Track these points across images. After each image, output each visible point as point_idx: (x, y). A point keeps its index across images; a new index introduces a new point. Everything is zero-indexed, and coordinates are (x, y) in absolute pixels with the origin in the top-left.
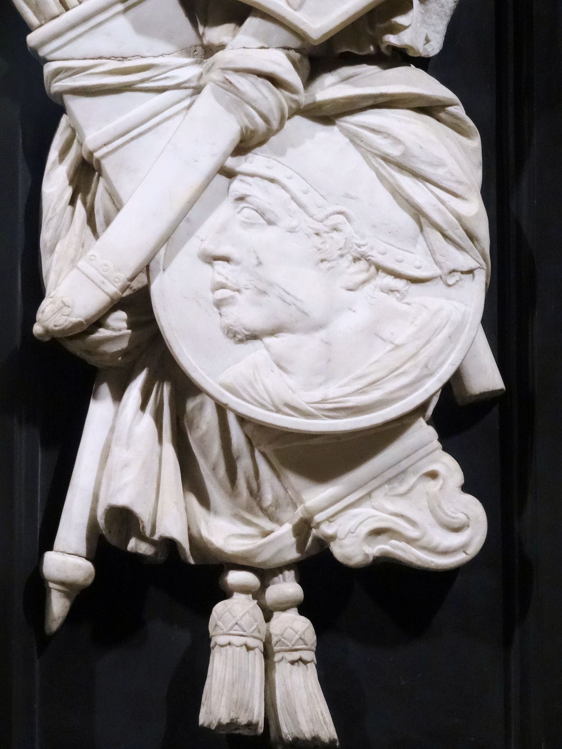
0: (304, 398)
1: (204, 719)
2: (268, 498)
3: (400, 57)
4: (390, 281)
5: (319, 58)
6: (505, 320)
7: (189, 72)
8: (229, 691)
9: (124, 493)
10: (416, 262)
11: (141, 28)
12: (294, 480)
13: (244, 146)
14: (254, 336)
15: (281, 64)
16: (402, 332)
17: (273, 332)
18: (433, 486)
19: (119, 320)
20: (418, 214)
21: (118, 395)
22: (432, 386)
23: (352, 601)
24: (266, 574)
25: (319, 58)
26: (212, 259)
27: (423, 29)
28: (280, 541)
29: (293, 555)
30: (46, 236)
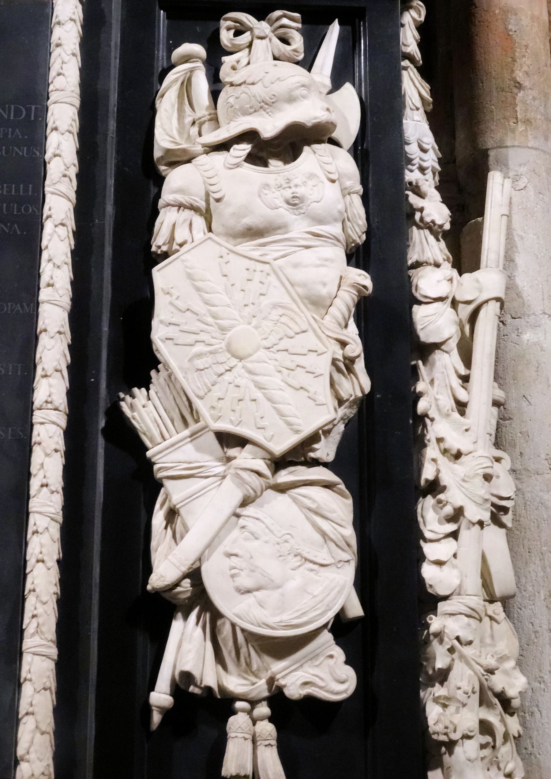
0: (272, 620)
1: (224, 773)
2: (255, 667)
3: (315, 463)
4: (311, 566)
5: (279, 463)
6: (364, 583)
7: (220, 469)
10: (323, 556)
11: (199, 449)
12: (267, 659)
13: (244, 503)
14: (249, 591)
15: (262, 466)
16: (317, 590)
17: (258, 589)
18: (331, 662)
19: (187, 583)
20: (324, 534)
21: (186, 617)
22: (330, 615)
23: (293, 716)
24: (253, 703)
25: (279, 463)
26: (230, 555)
27: (326, 450)
28: (261, 688)
29: (266, 694)
30: (153, 544)
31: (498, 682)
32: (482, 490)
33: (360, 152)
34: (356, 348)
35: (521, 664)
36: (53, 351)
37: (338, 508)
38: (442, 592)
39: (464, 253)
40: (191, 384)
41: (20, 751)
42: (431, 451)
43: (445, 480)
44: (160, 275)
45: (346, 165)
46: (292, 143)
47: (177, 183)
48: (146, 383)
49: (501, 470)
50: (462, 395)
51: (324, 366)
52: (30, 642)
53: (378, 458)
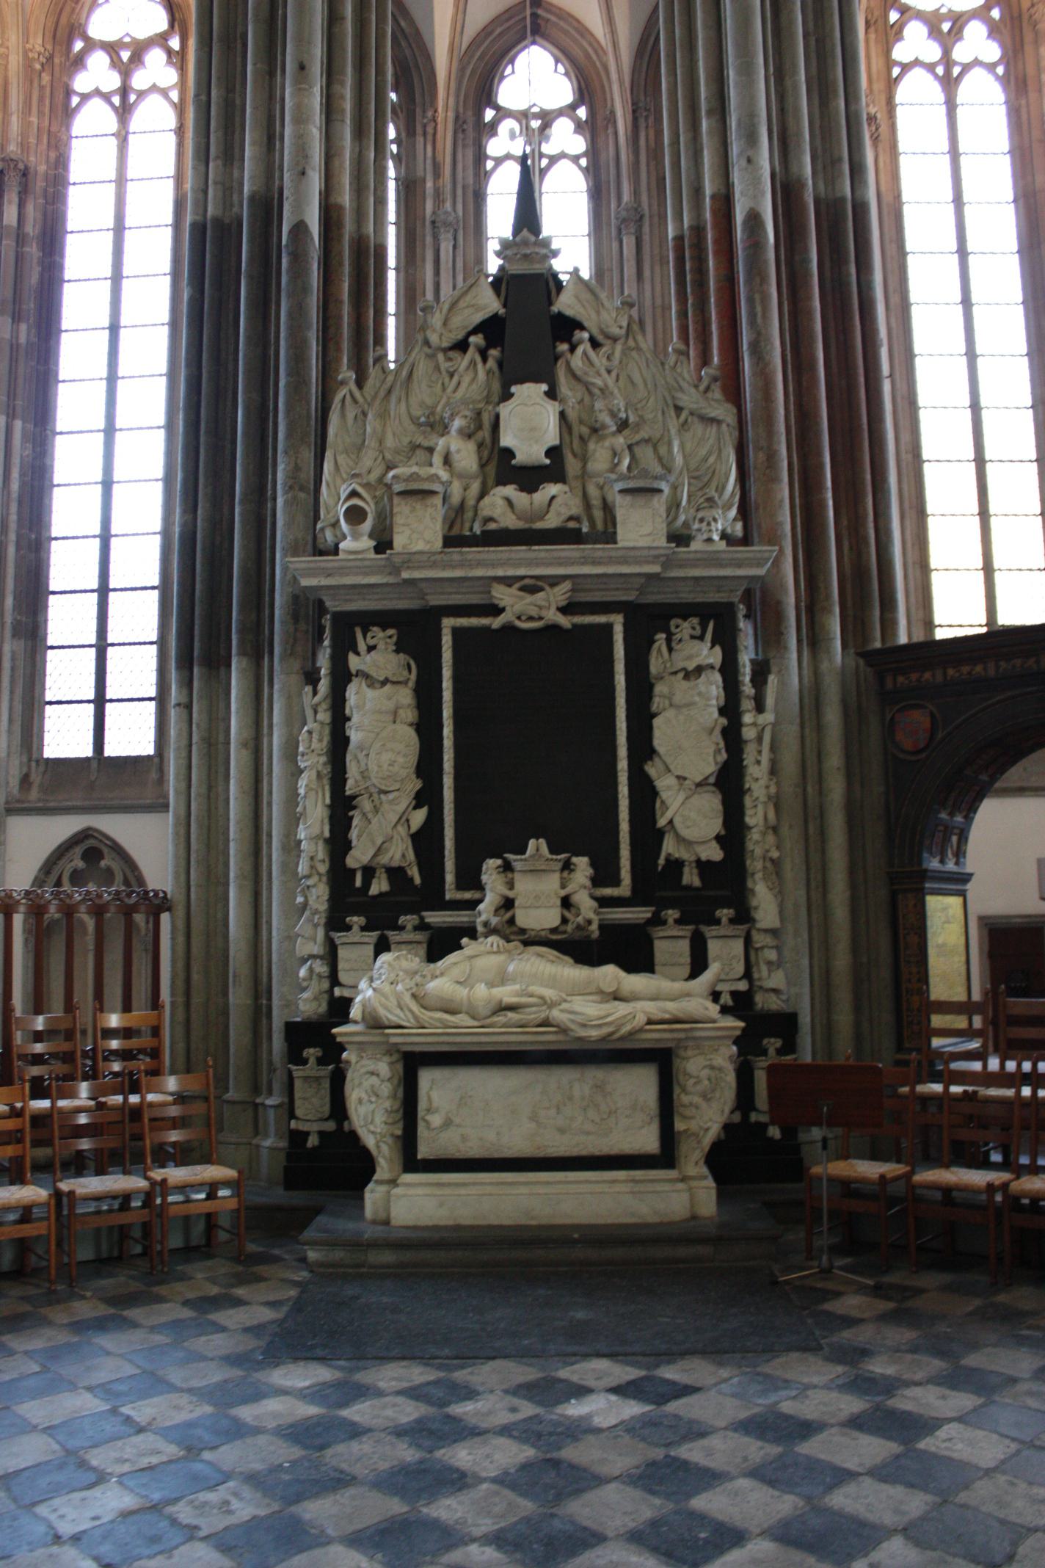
6: (726, 824)
8: (686, 879)
9: (670, 851)
23: (704, 867)
27: (712, 780)
28: (693, 858)
31: (770, 854)
33: (723, 670)
34: (722, 745)
35: (778, 848)
36: (622, 752)
39: (760, 708)
40: (668, 760)
42: (748, 778)
44: (657, 722)
45: (718, 677)
46: (699, 670)
47: (659, 689)
48: (651, 759)
51: (711, 750)
53: (729, 782)
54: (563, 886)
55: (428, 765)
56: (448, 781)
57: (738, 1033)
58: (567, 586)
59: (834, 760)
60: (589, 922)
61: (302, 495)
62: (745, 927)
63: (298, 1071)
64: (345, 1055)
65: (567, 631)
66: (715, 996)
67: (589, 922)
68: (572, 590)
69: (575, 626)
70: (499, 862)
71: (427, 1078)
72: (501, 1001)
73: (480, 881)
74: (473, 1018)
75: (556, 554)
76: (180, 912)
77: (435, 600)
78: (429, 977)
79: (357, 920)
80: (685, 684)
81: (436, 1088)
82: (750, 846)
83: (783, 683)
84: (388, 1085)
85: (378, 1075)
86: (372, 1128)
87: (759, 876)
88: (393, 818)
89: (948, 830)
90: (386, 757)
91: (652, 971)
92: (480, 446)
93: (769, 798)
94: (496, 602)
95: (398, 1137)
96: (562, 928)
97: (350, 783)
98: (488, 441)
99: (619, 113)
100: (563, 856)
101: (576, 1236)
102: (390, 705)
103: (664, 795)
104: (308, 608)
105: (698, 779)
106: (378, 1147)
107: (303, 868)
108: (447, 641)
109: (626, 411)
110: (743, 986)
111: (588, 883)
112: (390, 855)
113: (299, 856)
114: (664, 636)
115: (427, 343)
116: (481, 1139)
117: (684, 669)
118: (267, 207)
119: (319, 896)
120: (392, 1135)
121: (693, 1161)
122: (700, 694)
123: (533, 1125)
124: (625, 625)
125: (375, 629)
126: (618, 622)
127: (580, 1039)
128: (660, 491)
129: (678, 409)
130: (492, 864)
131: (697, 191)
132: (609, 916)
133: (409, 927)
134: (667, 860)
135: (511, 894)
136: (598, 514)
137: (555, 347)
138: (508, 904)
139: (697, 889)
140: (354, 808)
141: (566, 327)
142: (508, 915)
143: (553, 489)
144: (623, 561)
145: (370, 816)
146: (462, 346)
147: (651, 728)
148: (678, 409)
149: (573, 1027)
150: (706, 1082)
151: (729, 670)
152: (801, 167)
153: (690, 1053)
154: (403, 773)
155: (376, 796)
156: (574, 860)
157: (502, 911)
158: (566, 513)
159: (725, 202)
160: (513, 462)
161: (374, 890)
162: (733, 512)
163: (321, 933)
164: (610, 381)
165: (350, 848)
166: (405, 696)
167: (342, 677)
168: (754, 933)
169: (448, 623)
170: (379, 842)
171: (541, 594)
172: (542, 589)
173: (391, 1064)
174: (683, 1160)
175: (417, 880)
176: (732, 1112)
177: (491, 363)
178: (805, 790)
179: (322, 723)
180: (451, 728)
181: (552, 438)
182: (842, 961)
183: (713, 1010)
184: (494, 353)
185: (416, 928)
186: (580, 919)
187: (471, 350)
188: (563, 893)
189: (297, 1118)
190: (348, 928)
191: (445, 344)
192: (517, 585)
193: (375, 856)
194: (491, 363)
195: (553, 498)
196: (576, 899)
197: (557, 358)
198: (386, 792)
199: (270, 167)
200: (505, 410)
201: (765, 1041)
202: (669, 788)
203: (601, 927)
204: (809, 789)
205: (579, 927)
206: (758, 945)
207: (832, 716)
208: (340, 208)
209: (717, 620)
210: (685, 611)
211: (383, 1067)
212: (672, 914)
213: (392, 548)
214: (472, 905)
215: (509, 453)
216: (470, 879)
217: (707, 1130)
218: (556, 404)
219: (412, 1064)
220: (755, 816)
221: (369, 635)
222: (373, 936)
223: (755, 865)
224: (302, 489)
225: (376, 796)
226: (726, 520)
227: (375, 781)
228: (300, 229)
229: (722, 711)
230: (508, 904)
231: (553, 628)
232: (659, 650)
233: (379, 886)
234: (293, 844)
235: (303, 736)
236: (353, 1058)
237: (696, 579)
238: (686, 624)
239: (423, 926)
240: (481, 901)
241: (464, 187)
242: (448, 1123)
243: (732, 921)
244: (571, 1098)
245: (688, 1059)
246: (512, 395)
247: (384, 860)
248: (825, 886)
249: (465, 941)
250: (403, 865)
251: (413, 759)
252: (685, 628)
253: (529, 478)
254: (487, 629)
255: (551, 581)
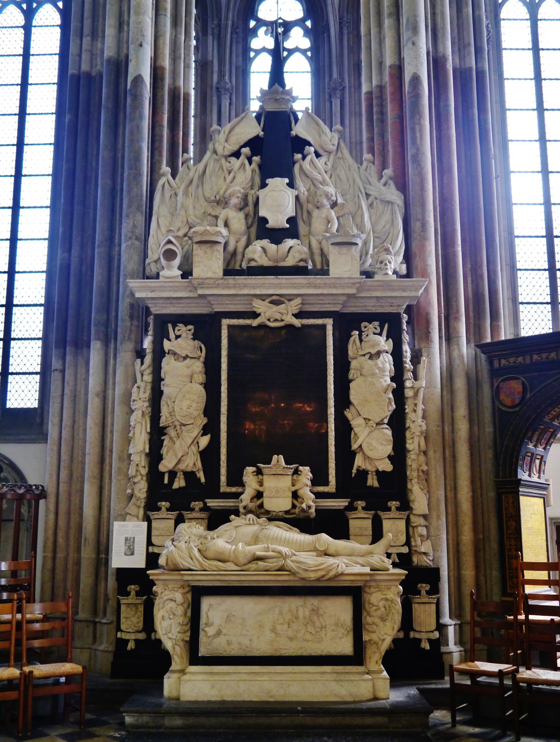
6: (394, 449)
9: (360, 465)
23: (380, 474)
27: (386, 421)
28: (374, 469)
31: (421, 468)
32: (419, 429)
37: (389, 432)
38: (410, 450)
39: (416, 378)
41: (330, 480)
43: (411, 426)
44: (352, 385)
46: (379, 353)
49: (423, 424)
50: (415, 408)
52: (330, 461)
53: (398, 422)
54: (293, 485)
55: (211, 409)
56: (224, 419)
57: (403, 577)
58: (298, 301)
59: (461, 411)
60: (309, 507)
61: (137, 243)
62: (407, 513)
63: (124, 601)
64: (155, 588)
65: (299, 328)
66: (389, 556)
67: (309, 507)
68: (302, 304)
69: (303, 326)
70: (254, 469)
71: (206, 603)
72: (255, 554)
73: (242, 481)
74: (237, 565)
75: (292, 281)
76: (52, 499)
77: (218, 309)
78: (210, 538)
79: (164, 504)
80: (370, 362)
81: (213, 609)
82: (409, 462)
83: (430, 363)
84: (182, 607)
85: (175, 601)
86: (170, 635)
87: (415, 481)
88: (190, 441)
89: (533, 457)
90: (185, 404)
91: (349, 539)
92: (247, 216)
93: (422, 432)
94: (255, 310)
95: (186, 641)
96: (293, 511)
97: (163, 419)
98: (252, 213)
99: (332, 23)
100: (294, 465)
101: (299, 708)
102: (188, 372)
103: (356, 430)
104: (141, 311)
105: (378, 420)
106: (174, 648)
107: (132, 471)
108: (224, 333)
109: (336, 196)
110: (405, 550)
111: (309, 483)
112: (186, 464)
113: (129, 464)
114: (357, 332)
115: (215, 152)
116: (239, 643)
117: (370, 353)
118: (120, 66)
119: (141, 489)
120: (183, 640)
121: (374, 659)
122: (379, 368)
123: (273, 635)
124: (333, 326)
125: (180, 325)
126: (329, 323)
127: (303, 579)
128: (357, 244)
129: (368, 195)
130: (250, 470)
131: (381, 64)
132: (321, 504)
133: (197, 509)
134: (357, 470)
135: (261, 489)
136: (318, 259)
137: (293, 156)
138: (259, 495)
139: (376, 488)
140: (165, 434)
141: (300, 144)
142: (260, 502)
143: (290, 242)
144: (335, 286)
145: (175, 439)
146: (237, 154)
147: (349, 388)
148: (368, 195)
149: (299, 571)
150: (383, 609)
151: (397, 354)
152: (445, 48)
153: (372, 590)
154: (196, 413)
155: (178, 427)
156: (301, 468)
157: (255, 500)
158: (298, 257)
159: (398, 70)
160: (267, 226)
161: (176, 486)
162: (401, 258)
163: (141, 512)
164: (327, 177)
165: (162, 459)
166: (198, 366)
167: (159, 354)
168: (412, 518)
169: (225, 322)
170: (180, 456)
171: (283, 306)
172: (283, 303)
173: (184, 594)
174: (368, 659)
175: (203, 480)
176: (399, 631)
177: (254, 165)
178: (443, 429)
179: (146, 382)
180: (226, 386)
181: (290, 211)
182: (467, 536)
183: (388, 563)
184: (256, 159)
185: (201, 510)
186: (304, 506)
187: (242, 157)
188: (294, 489)
189: (122, 631)
190: (159, 509)
191: (227, 153)
192: (268, 300)
193: (177, 464)
194: (254, 165)
195: (291, 247)
196: (300, 493)
197: (294, 163)
198: (185, 425)
199: (122, 41)
200: (262, 193)
201: (419, 585)
202: (359, 425)
203: (316, 510)
204: (446, 429)
205: (303, 510)
206: (413, 525)
207: (460, 384)
208: (163, 68)
209: (390, 323)
210: (370, 317)
211: (178, 596)
212: (361, 504)
213: (192, 276)
214: (237, 496)
215: (264, 220)
216: (236, 479)
217: (384, 640)
218: (294, 190)
219: (198, 593)
220: (413, 444)
221: (177, 328)
222: (173, 515)
223: (412, 473)
224: (137, 239)
225: (178, 427)
226: (395, 263)
227: (178, 418)
228: (138, 79)
229: (392, 379)
230: (259, 495)
231: (290, 327)
232: (354, 341)
233: (179, 483)
234: (125, 456)
235: (135, 389)
236: (159, 592)
237: (377, 298)
238: (371, 326)
239: (205, 508)
240: (242, 493)
241: (237, 68)
242: (219, 633)
243: (398, 509)
244: (297, 618)
245: (371, 594)
246: (267, 185)
247: (182, 467)
248: (455, 489)
249: (232, 517)
250: (194, 470)
251: (202, 405)
252: (371, 328)
253: (277, 235)
254: (249, 327)
255: (289, 298)
